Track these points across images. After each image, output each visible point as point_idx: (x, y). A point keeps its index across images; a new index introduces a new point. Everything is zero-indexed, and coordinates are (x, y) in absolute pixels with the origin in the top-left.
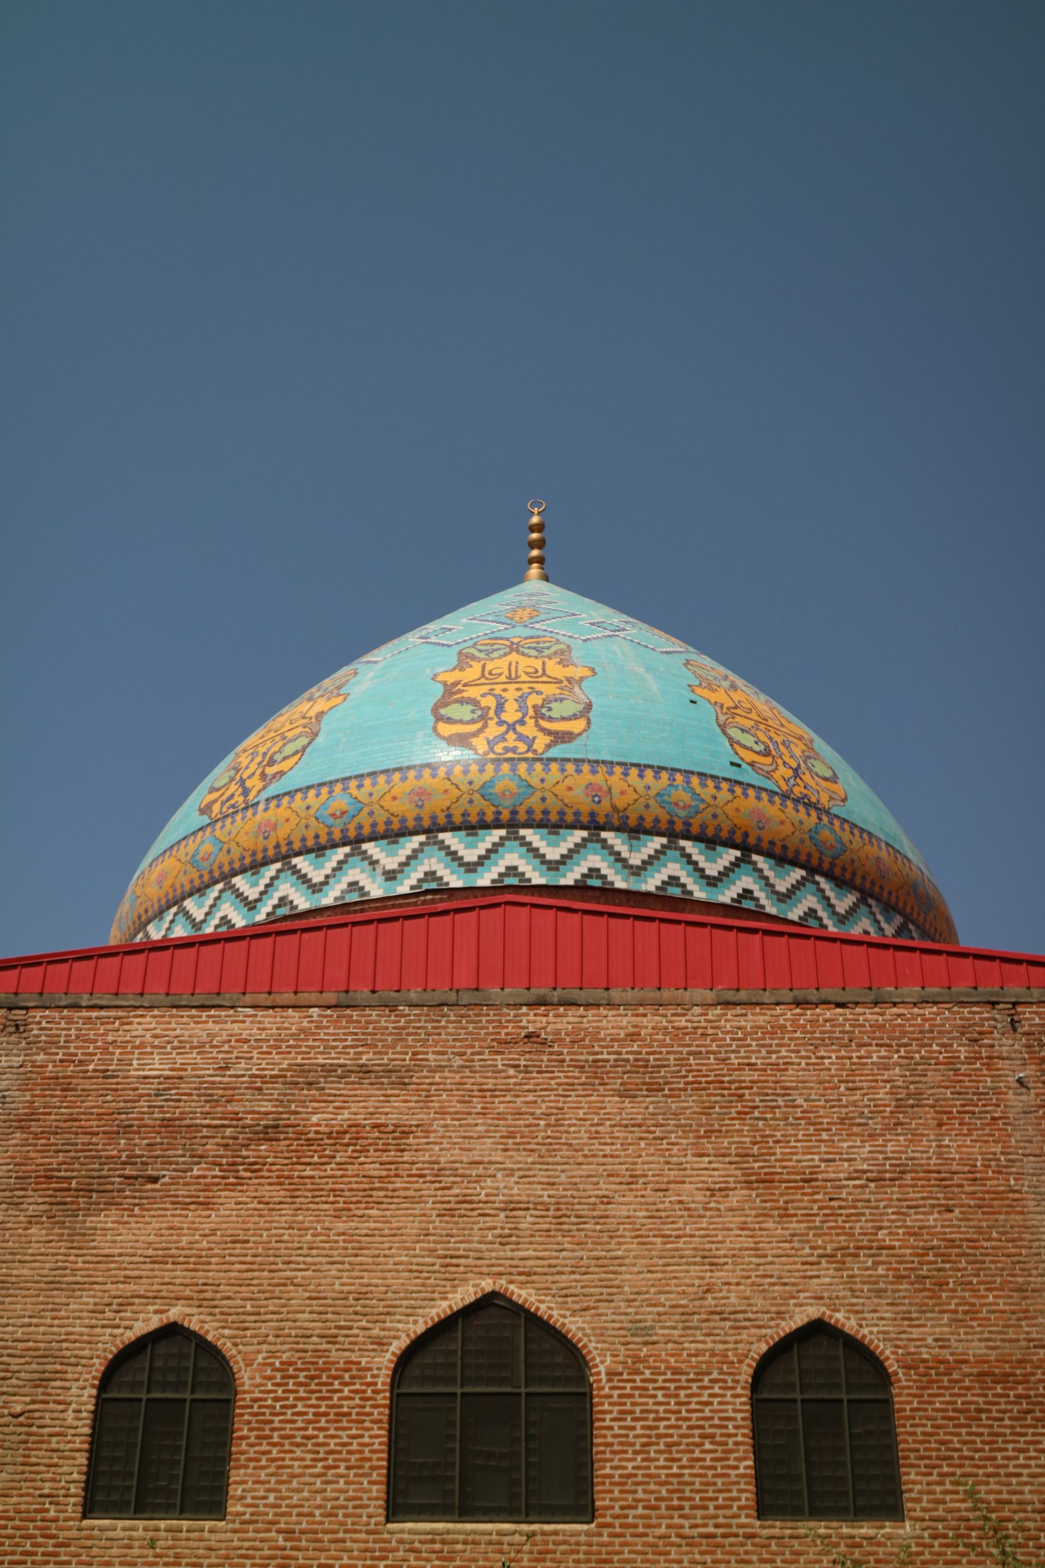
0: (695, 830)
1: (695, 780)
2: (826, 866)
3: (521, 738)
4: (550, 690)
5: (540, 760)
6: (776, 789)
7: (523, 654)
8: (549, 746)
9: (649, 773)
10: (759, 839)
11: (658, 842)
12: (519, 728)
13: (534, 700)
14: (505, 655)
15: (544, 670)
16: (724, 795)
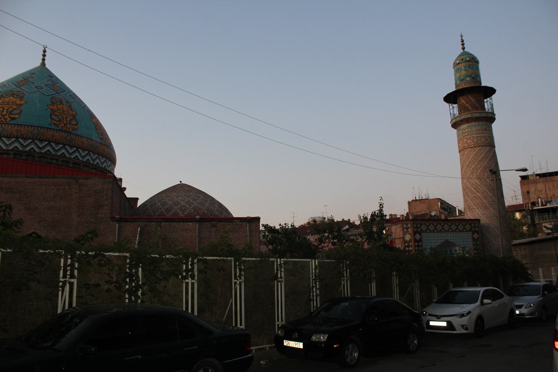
0: (38, 138)
1: (39, 128)
2: (68, 143)
3: (5, 119)
4: (15, 107)
5: (7, 124)
6: (59, 129)
7: (14, 97)
8: (10, 121)
9: (30, 127)
10: (52, 140)
11: (30, 141)
12: (5, 116)
13: (10, 109)
14: (10, 96)
15: (16, 101)
16: (46, 131)
